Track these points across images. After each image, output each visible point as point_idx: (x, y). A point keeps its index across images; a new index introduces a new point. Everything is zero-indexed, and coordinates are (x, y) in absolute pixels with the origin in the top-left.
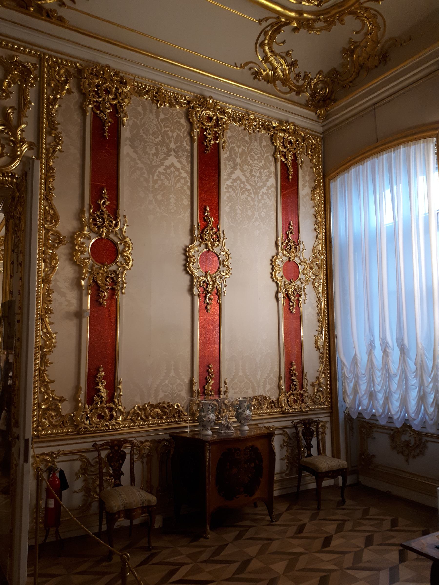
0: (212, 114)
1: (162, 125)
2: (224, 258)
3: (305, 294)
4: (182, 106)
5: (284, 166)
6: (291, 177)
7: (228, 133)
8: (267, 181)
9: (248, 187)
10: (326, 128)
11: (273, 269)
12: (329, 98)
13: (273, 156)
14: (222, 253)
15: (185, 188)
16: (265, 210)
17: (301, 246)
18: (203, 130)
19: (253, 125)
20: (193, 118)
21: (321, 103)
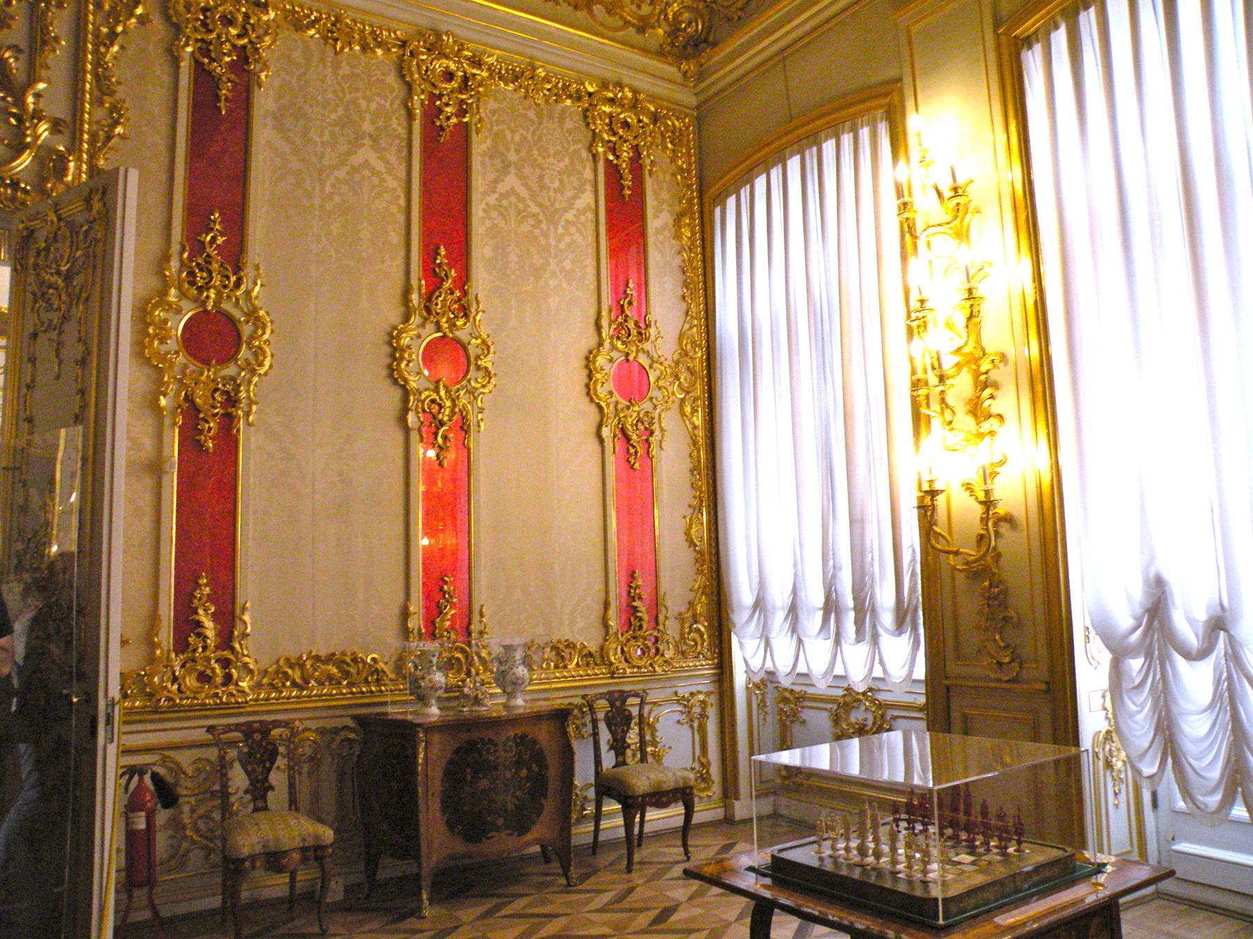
0: (453, 67)
1: (346, 86)
2: (479, 351)
3: (662, 430)
4: (389, 50)
5: (613, 171)
6: (628, 192)
7: (488, 106)
8: (576, 197)
9: (534, 209)
10: (702, 98)
11: (590, 377)
12: (706, 41)
13: (589, 149)
14: (473, 341)
15: (394, 209)
16: (571, 256)
17: (652, 331)
18: (433, 97)
19: (543, 89)
20: (412, 74)
21: (690, 50)
